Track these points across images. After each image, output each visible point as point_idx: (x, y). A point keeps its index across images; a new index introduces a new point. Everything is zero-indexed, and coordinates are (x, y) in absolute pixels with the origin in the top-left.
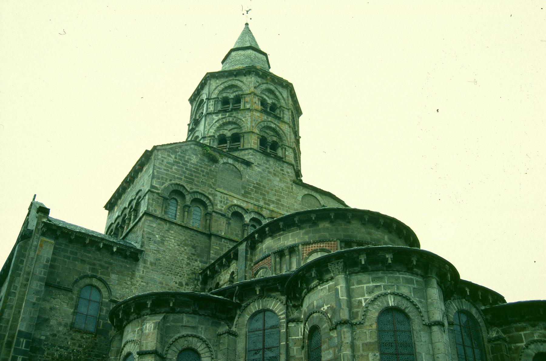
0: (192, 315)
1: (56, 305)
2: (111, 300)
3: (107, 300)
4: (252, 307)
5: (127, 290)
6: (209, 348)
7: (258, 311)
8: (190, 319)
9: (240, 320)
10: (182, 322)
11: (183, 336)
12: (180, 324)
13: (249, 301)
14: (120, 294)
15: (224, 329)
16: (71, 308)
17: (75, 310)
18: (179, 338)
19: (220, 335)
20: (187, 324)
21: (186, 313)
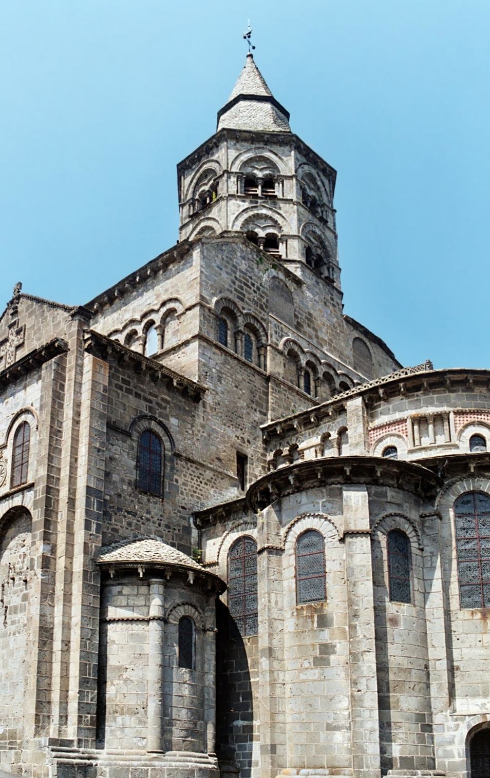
0: (396, 489)
1: (116, 454)
2: (175, 453)
3: (170, 454)
4: (459, 487)
5: (189, 442)
6: (416, 531)
7: (468, 492)
8: (394, 494)
9: (443, 501)
10: (386, 497)
11: (391, 515)
12: (384, 500)
13: (454, 479)
14: (182, 446)
15: (429, 510)
16: (133, 459)
17: (137, 462)
18: (387, 516)
19: (426, 516)
20: (393, 500)
21: (389, 487)
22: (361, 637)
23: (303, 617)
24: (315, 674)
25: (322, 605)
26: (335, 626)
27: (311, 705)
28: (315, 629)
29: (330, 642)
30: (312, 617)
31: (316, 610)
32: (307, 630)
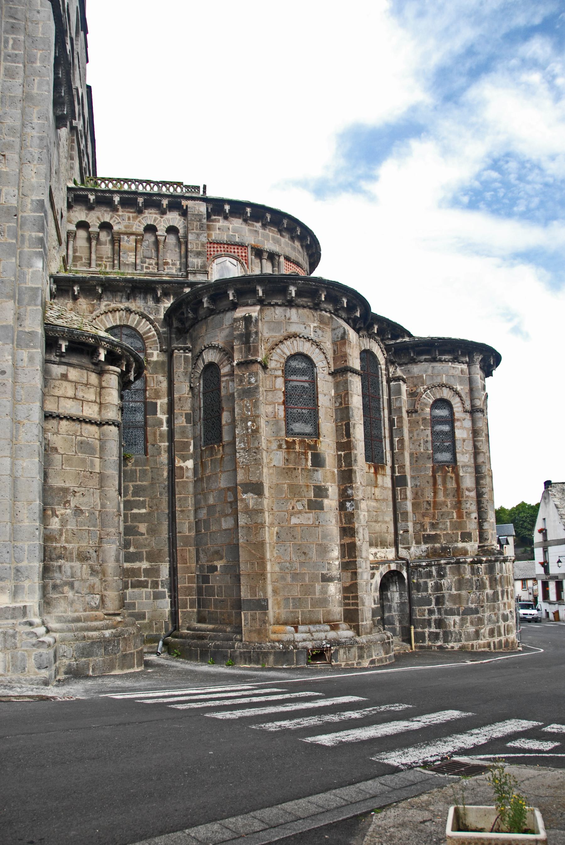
22: (359, 483)
23: (295, 452)
24: (309, 519)
25: (316, 441)
26: (328, 468)
27: (304, 553)
28: (309, 468)
29: (323, 484)
30: (305, 454)
31: (310, 447)
32: (300, 468)
